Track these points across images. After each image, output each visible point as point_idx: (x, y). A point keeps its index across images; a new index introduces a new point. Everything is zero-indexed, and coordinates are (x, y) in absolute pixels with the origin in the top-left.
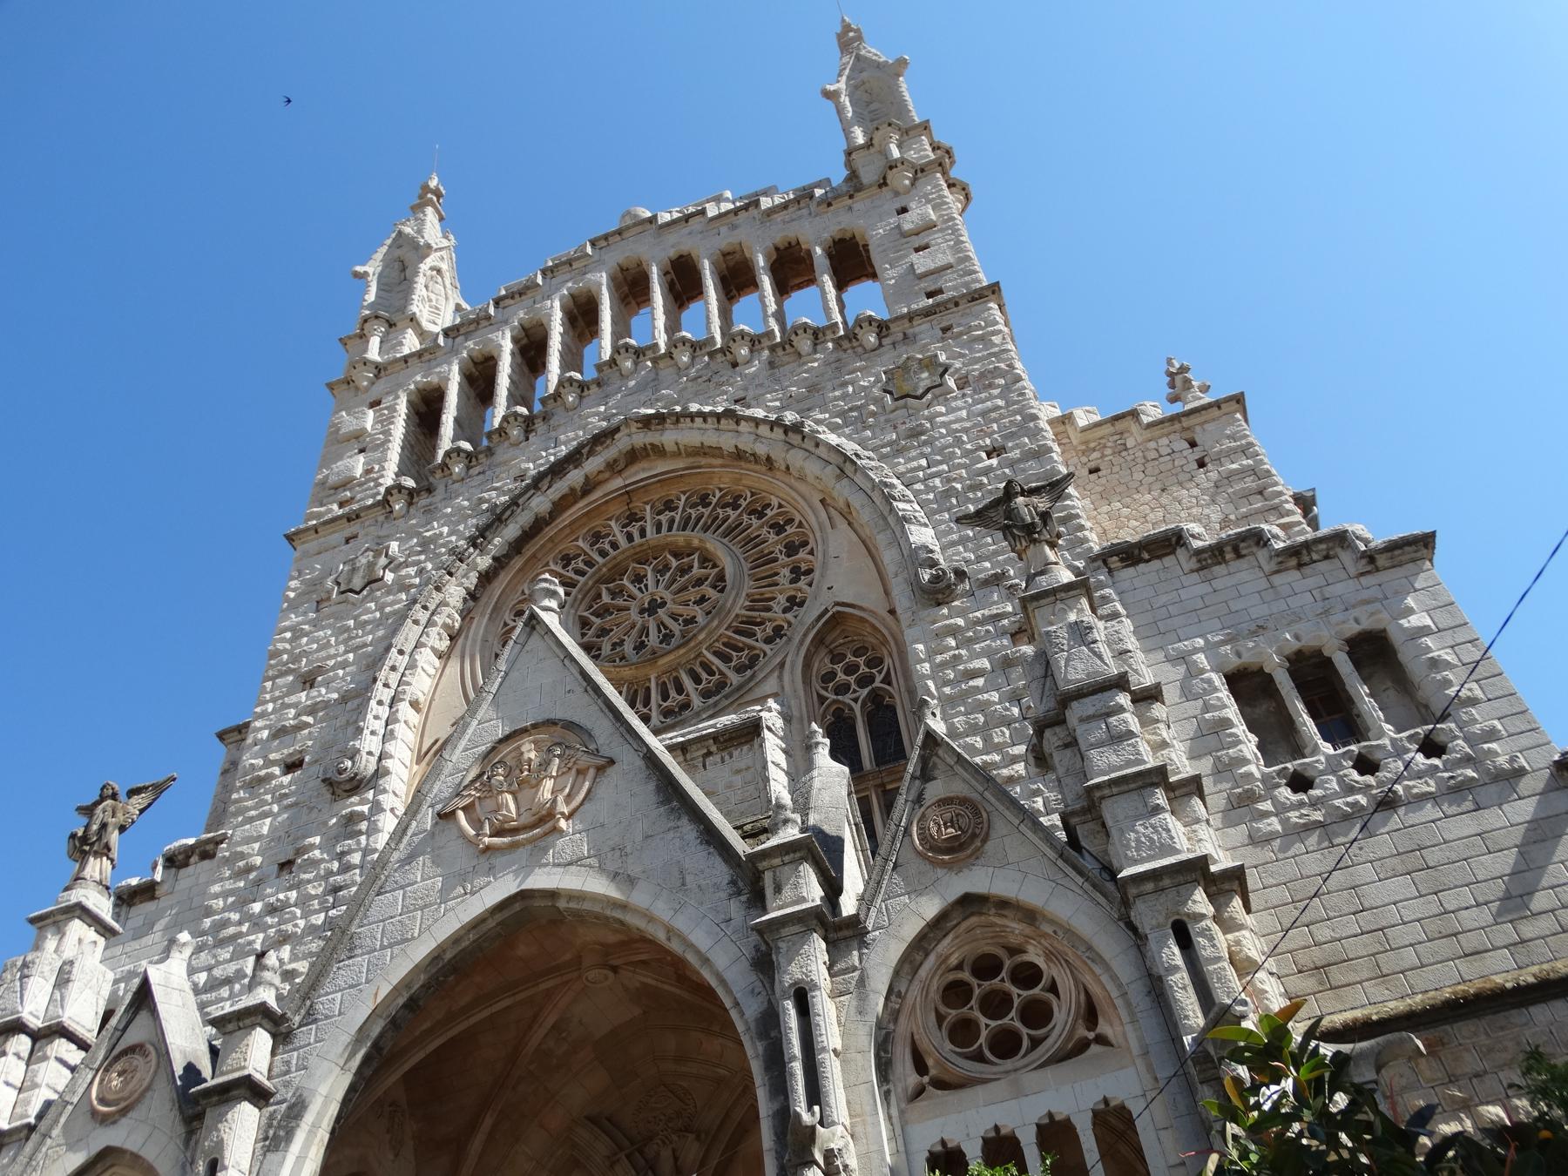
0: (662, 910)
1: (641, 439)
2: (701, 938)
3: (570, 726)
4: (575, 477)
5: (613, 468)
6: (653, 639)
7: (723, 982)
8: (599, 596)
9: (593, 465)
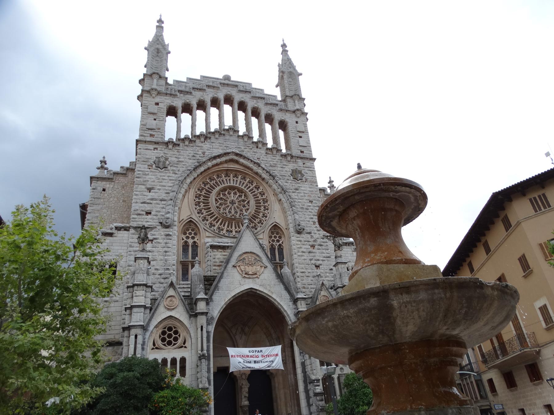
0: (278, 300)
2: (285, 307)
3: (258, 255)
4: (218, 160)
5: (226, 162)
6: (233, 212)
7: (288, 315)
8: (219, 194)
9: (223, 159)
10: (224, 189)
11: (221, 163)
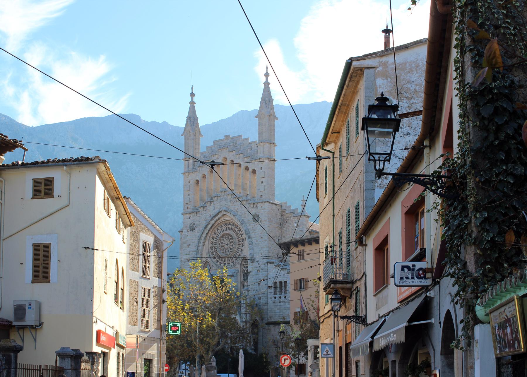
1: (225, 213)
4: (217, 218)
9: (219, 216)
10: (223, 236)
11: (219, 219)
